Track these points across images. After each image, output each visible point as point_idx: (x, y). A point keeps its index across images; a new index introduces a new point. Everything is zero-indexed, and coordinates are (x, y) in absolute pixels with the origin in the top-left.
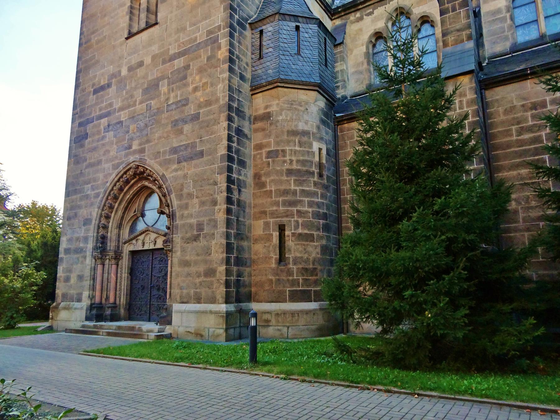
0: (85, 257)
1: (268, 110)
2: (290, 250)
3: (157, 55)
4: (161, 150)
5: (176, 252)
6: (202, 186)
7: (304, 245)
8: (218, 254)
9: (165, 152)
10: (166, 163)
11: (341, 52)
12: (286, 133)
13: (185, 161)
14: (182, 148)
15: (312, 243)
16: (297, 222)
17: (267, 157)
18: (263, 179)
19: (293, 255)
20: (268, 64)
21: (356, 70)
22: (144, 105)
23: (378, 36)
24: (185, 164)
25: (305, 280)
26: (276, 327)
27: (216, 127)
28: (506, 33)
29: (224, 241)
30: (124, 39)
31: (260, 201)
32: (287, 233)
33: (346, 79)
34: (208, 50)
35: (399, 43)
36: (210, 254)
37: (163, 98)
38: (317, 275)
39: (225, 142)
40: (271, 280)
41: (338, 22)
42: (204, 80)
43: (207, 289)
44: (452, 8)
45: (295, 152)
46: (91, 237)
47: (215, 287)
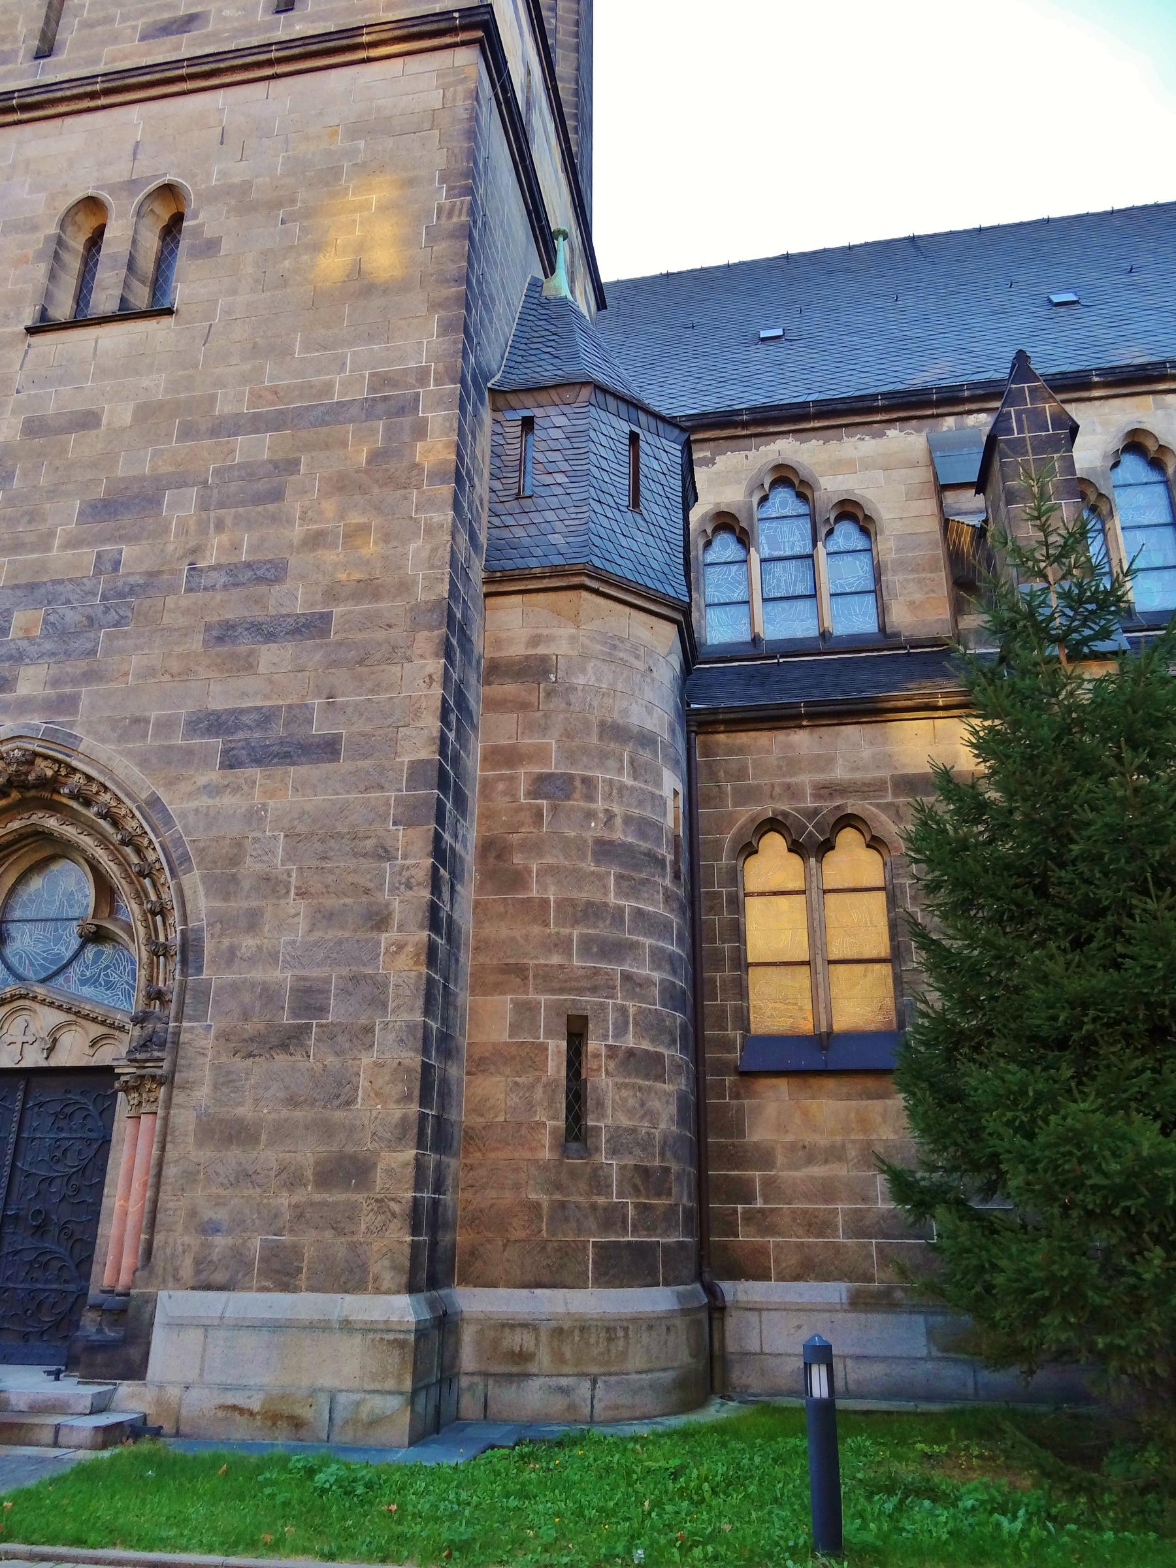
1: (541, 650)
2: (600, 1104)
3: (161, 405)
4: (153, 715)
5: (187, 1086)
6: (324, 858)
7: (640, 1089)
8: (380, 1105)
9: (165, 726)
10: (169, 761)
12: (595, 731)
13: (258, 762)
14: (245, 719)
15: (659, 1085)
16: (623, 1011)
17: (534, 794)
18: (517, 859)
19: (609, 1121)
20: (550, 516)
22: (88, 555)
24: (256, 773)
25: (643, 1208)
26: (553, 1382)
27: (396, 669)
29: (413, 1059)
30: (22, 328)
31: (500, 931)
32: (594, 1045)
34: (374, 432)
35: (1051, 539)
36: (348, 1103)
37: (173, 544)
38: (669, 1194)
39: (433, 724)
40: (537, 1206)
42: (356, 518)
43: (328, 1234)
45: (622, 788)
47: (363, 1227)
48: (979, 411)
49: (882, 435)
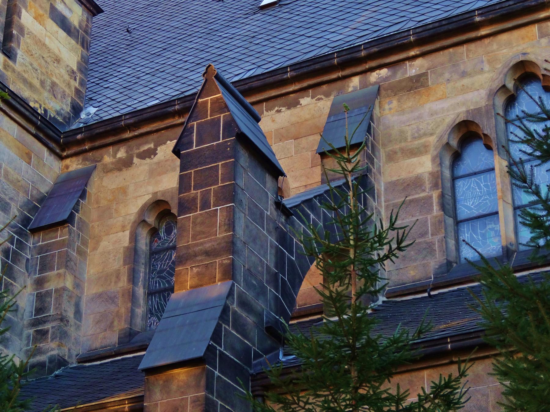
11: (62, 244)
21: (101, 290)
23: (162, 213)
28: (429, 238)
33: (70, 314)
41: (75, 165)
44: (201, 200)
48: (380, 67)
49: (296, 104)
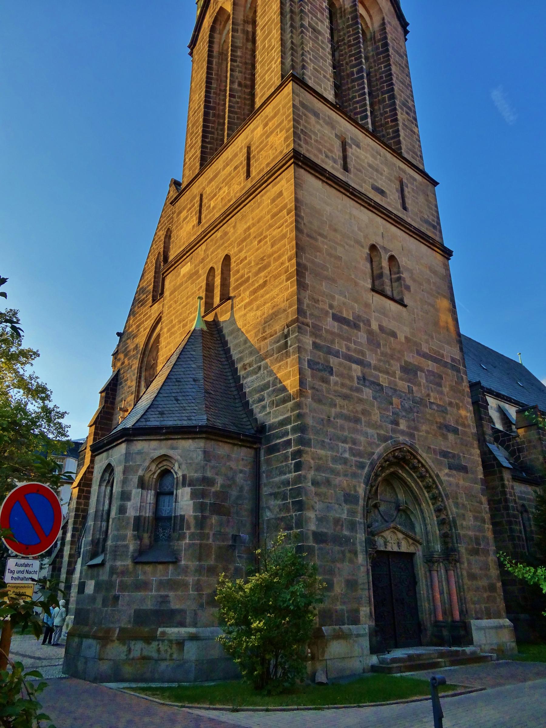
0: (355, 553)
14: (450, 455)
46: (360, 523)
